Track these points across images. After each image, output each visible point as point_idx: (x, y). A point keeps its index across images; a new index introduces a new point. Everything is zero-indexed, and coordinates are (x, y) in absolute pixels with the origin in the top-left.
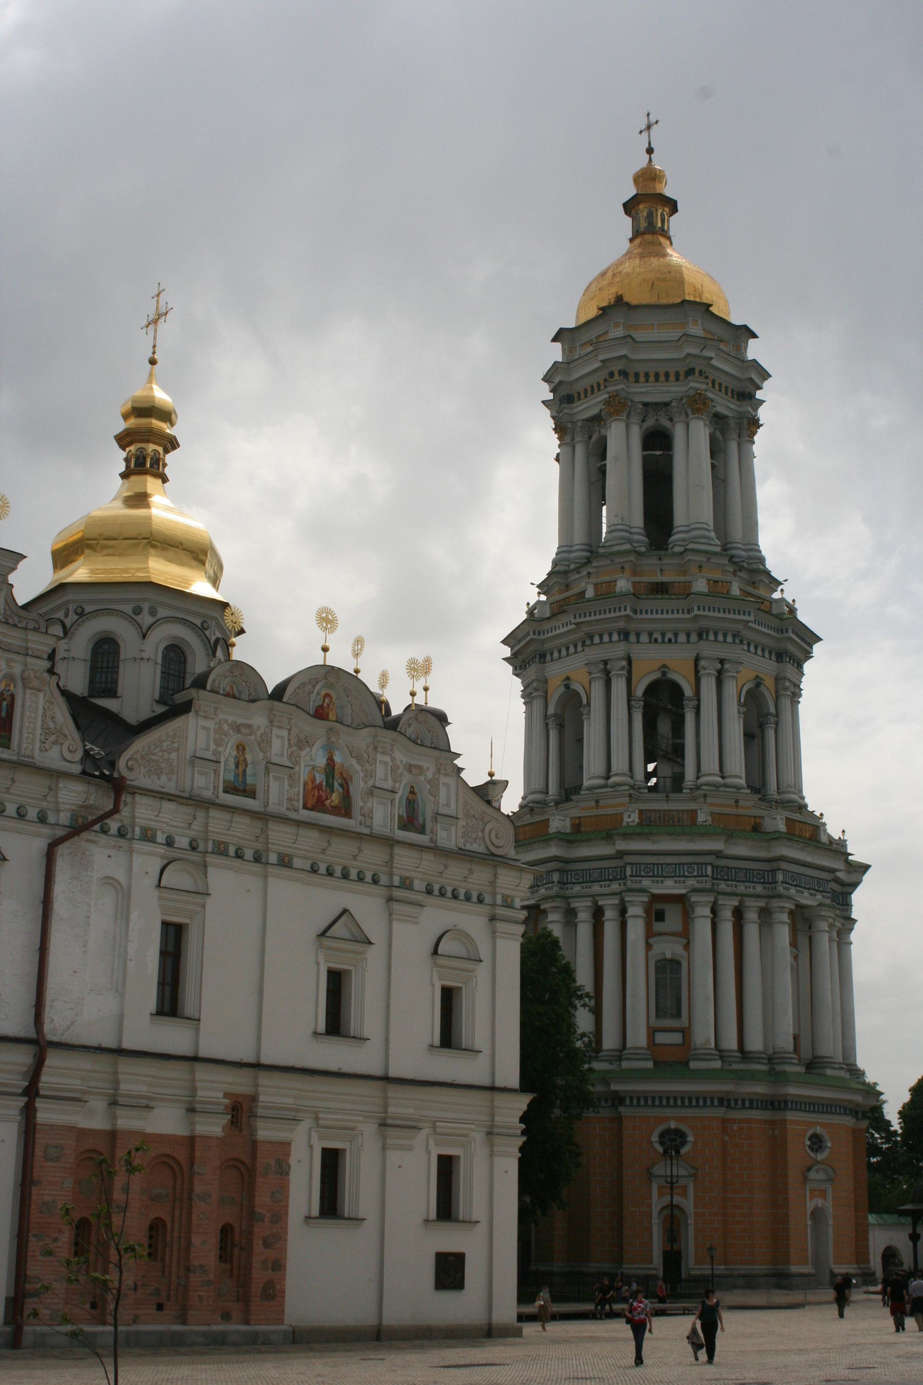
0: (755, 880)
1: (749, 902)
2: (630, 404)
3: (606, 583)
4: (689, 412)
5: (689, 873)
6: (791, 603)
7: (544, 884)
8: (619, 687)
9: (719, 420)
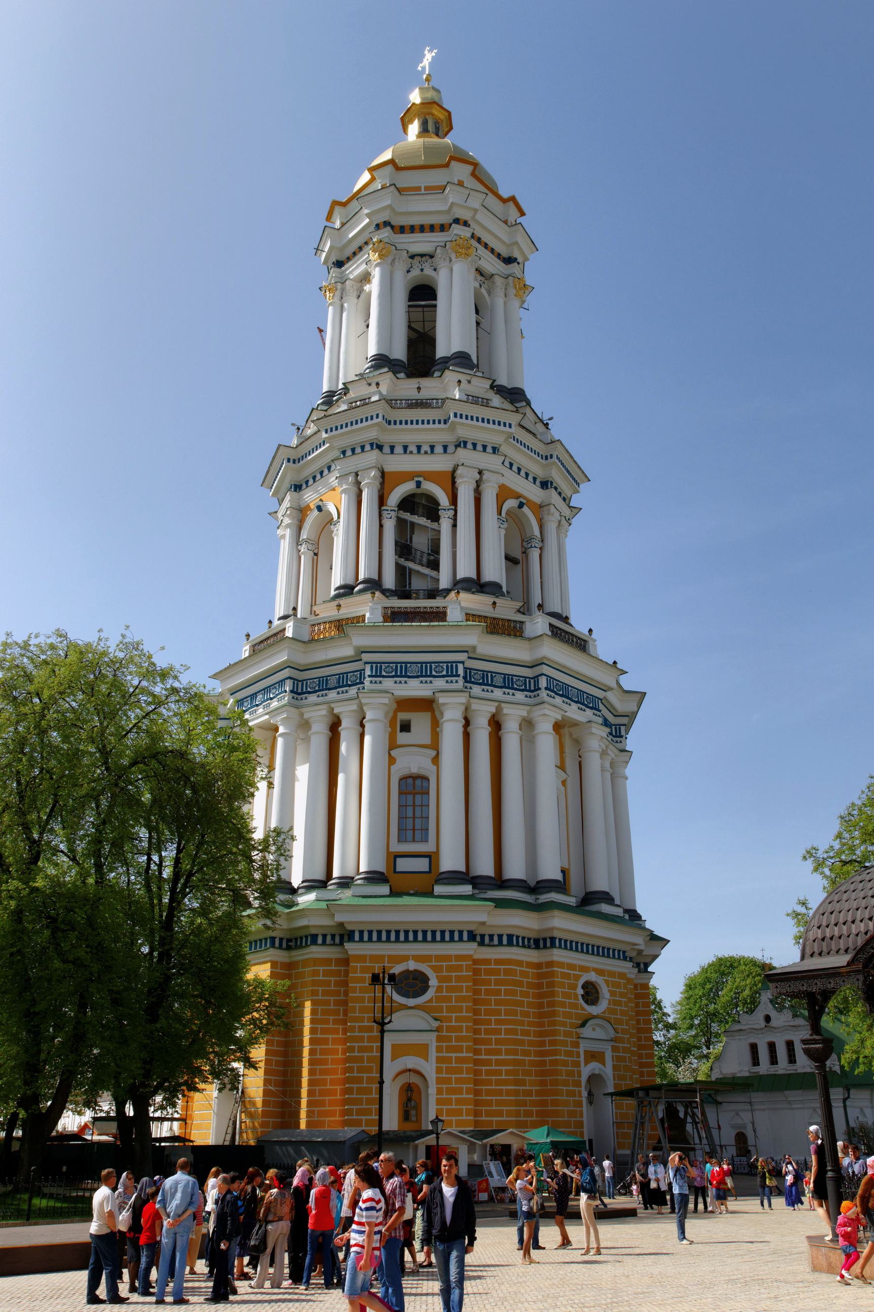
0: (515, 686)
5: (436, 672)
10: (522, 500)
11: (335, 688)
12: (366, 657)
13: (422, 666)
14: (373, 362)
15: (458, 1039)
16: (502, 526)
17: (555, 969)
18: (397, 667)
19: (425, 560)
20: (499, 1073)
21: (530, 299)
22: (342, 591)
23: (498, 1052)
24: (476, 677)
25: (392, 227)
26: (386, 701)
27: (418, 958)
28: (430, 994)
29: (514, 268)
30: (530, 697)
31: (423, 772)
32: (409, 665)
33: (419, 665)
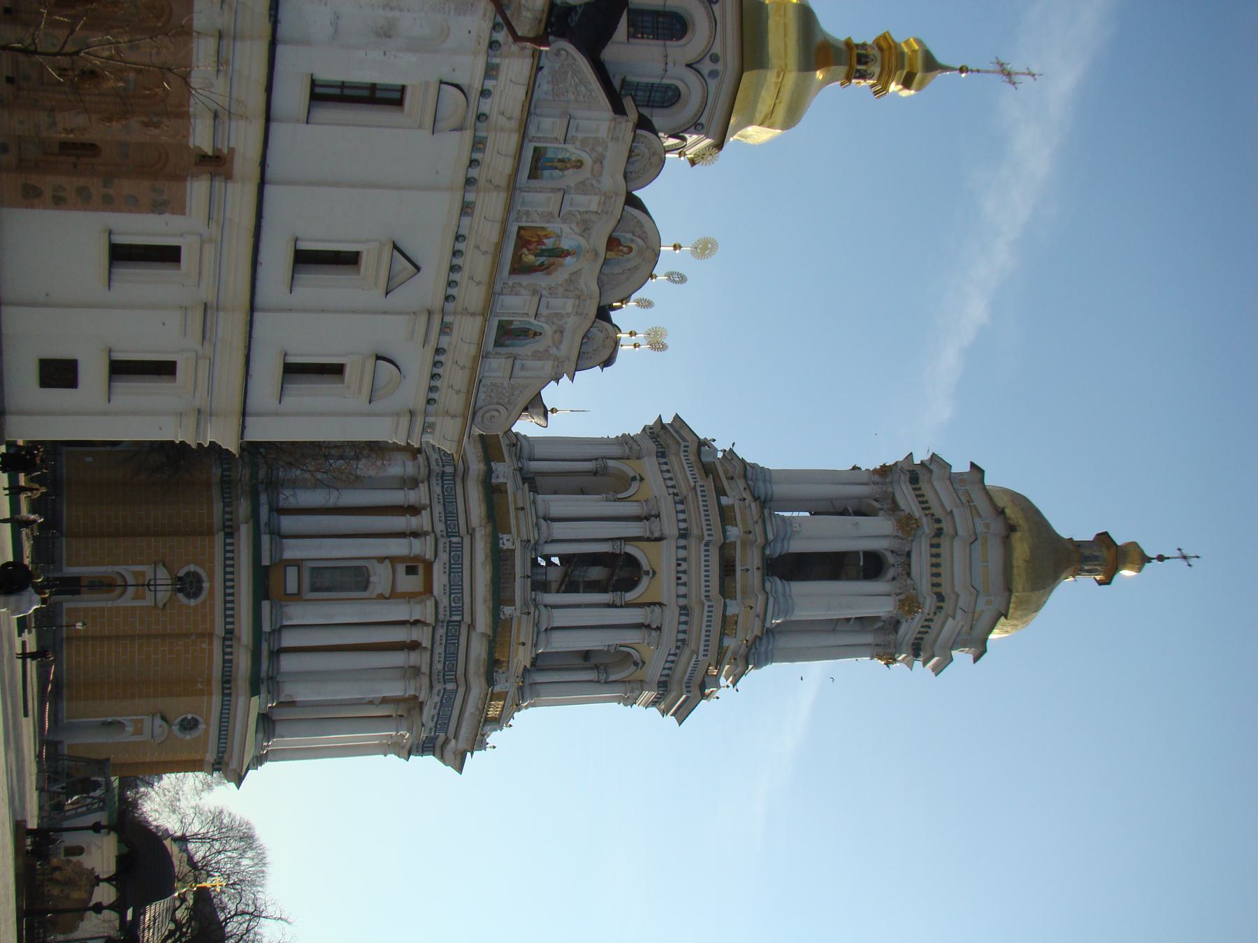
0: (447, 663)
1: (427, 656)
2: (909, 539)
4: (902, 597)
5: (454, 598)
6: (715, 696)
8: (633, 529)
9: (895, 624)
10: (641, 665)
27: (212, 588)
33: (460, 583)
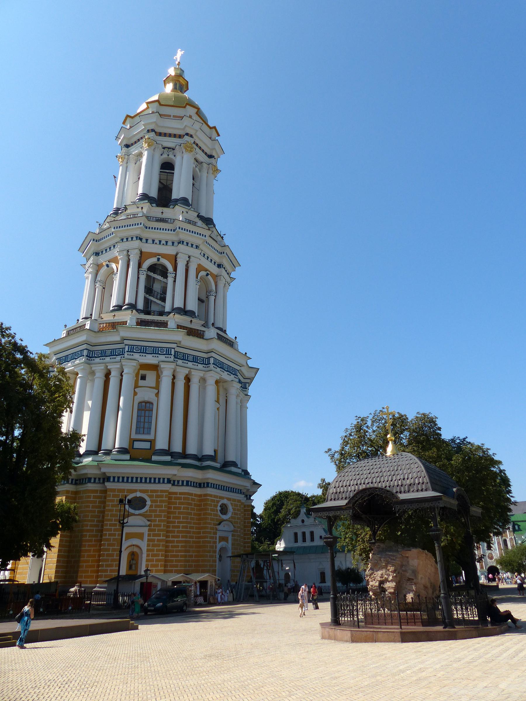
0: (198, 362)
3: (133, 215)
4: (184, 151)
7: (80, 357)
10: (208, 272)
11: (109, 356)
12: (126, 342)
13: (154, 349)
14: (140, 197)
15: (159, 530)
16: (198, 284)
17: (208, 497)
18: (141, 348)
19: (159, 297)
20: (178, 546)
21: (219, 176)
22: (116, 308)
23: (178, 537)
24: (180, 356)
25: (156, 132)
26: (135, 364)
27: (141, 491)
28: (147, 508)
29: (212, 160)
30: (205, 367)
31: (151, 400)
32: (147, 348)
